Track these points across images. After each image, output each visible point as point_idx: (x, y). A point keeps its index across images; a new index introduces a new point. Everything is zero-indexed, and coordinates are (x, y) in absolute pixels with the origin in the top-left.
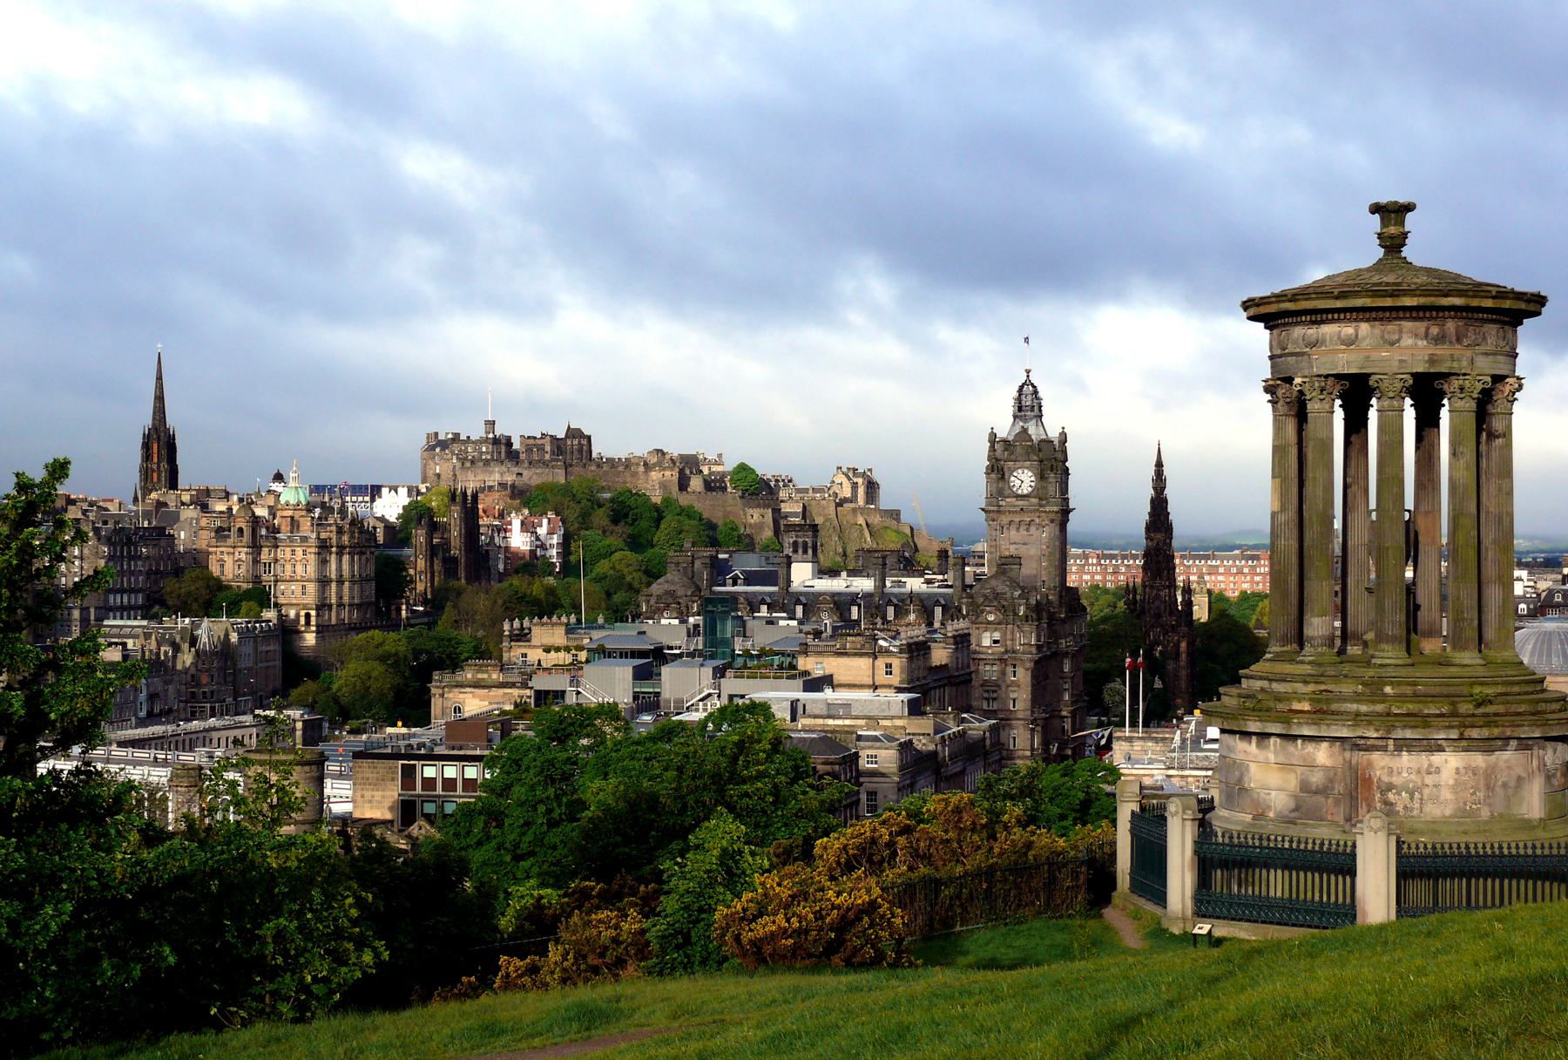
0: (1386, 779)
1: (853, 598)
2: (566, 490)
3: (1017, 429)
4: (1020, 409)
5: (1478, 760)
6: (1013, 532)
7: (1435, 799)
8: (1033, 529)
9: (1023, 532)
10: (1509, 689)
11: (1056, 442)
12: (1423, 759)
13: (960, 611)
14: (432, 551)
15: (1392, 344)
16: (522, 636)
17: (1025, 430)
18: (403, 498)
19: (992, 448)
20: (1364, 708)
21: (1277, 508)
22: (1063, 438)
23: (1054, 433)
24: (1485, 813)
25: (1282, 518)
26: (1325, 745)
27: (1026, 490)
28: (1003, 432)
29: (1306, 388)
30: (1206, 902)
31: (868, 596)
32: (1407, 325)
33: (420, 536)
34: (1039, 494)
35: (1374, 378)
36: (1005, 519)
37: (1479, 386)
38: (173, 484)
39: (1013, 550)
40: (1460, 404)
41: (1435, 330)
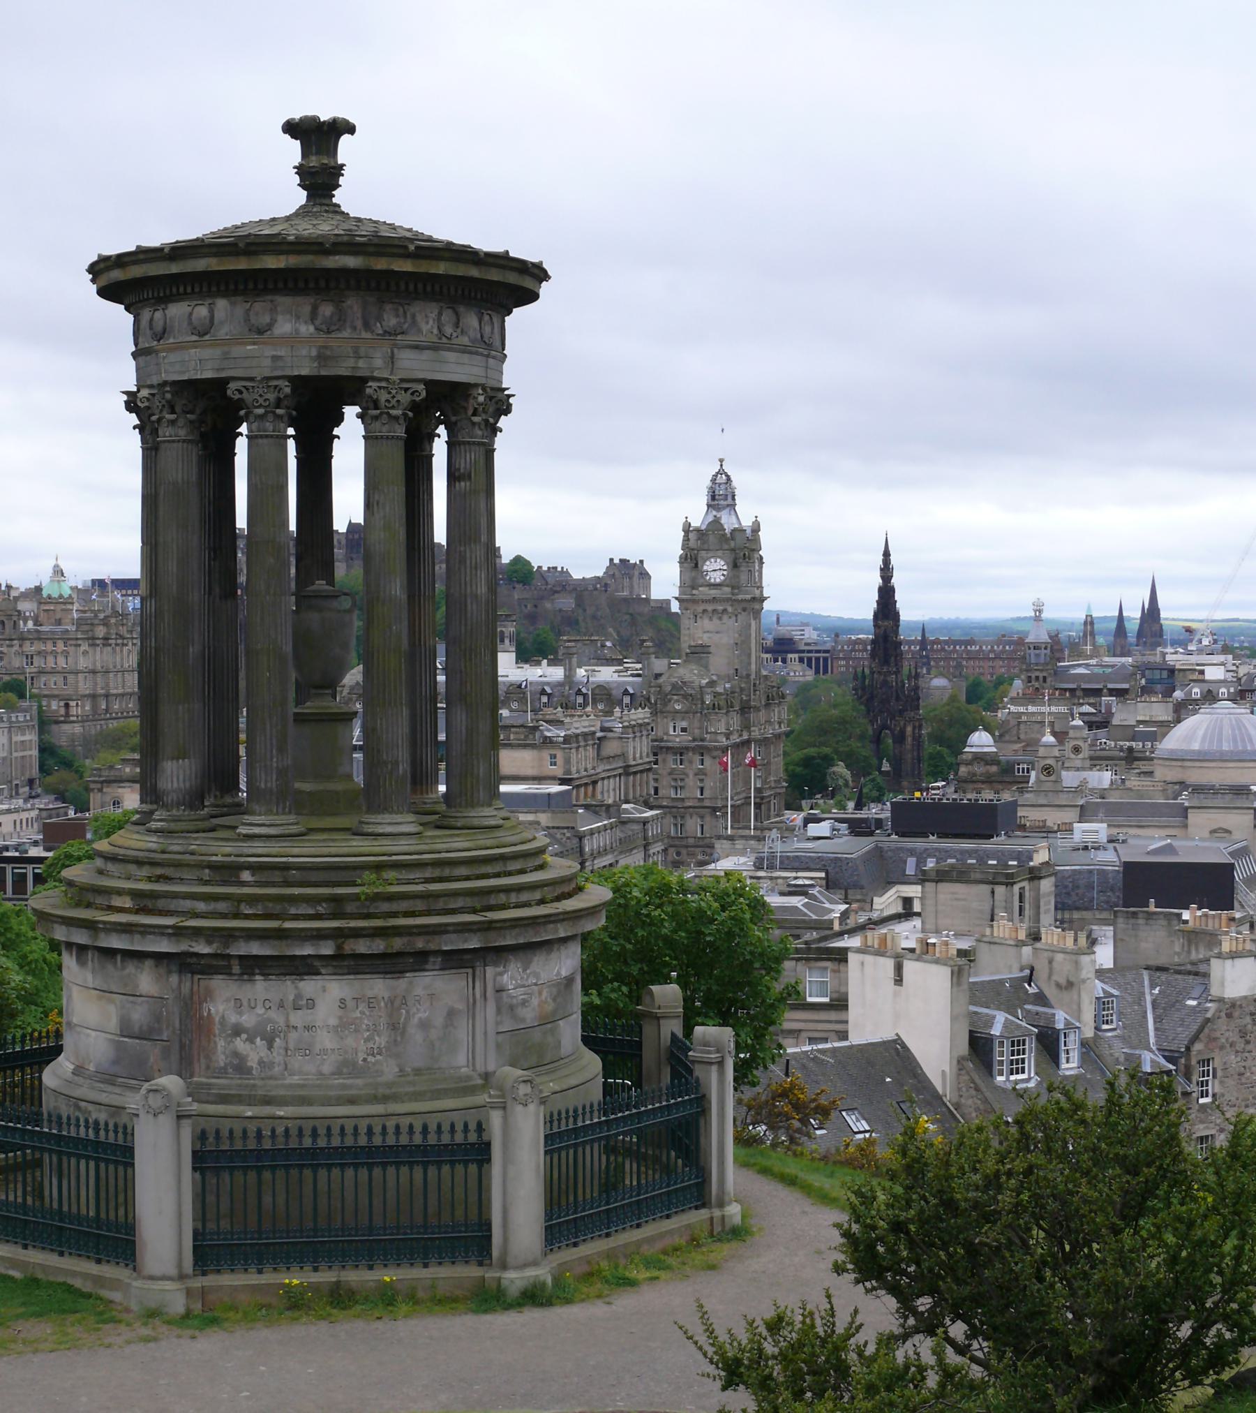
0: (233, 1018)
3: (710, 519)
4: (713, 498)
5: (378, 987)
6: (706, 621)
7: (306, 1050)
8: (725, 617)
9: (716, 621)
10: (447, 872)
11: (749, 532)
12: (287, 988)
13: (648, 699)
15: (260, 332)
17: (717, 521)
19: (686, 539)
22: (756, 528)
23: (747, 522)
24: (389, 1070)
26: (149, 963)
27: (717, 577)
28: (696, 522)
31: (560, 684)
32: (284, 301)
34: (733, 583)
35: (233, 386)
36: (700, 608)
37: (405, 398)
39: (704, 639)
41: (327, 310)
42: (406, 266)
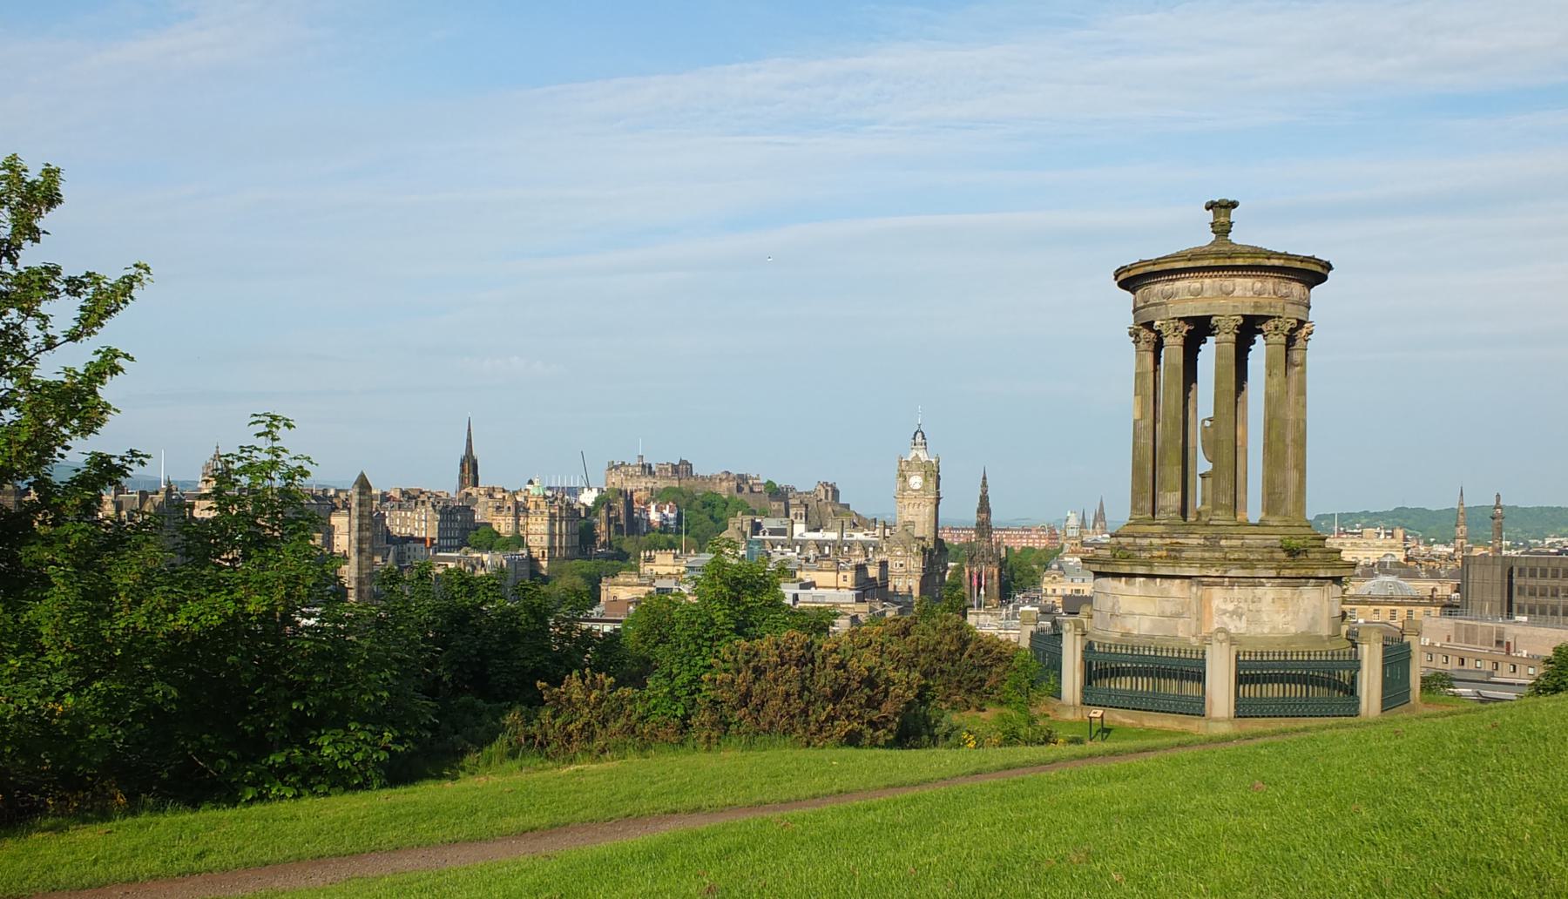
1: (826, 543)
2: (679, 491)
5: (1288, 591)
14: (609, 521)
16: (650, 560)
18: (595, 494)
20: (1207, 555)
21: (1137, 416)
25: (1142, 424)
26: (1178, 581)
27: (917, 487)
29: (1163, 329)
30: (1088, 699)
33: (603, 513)
34: (924, 488)
38: (476, 485)
40: (1273, 339)
42: (1298, 265)
